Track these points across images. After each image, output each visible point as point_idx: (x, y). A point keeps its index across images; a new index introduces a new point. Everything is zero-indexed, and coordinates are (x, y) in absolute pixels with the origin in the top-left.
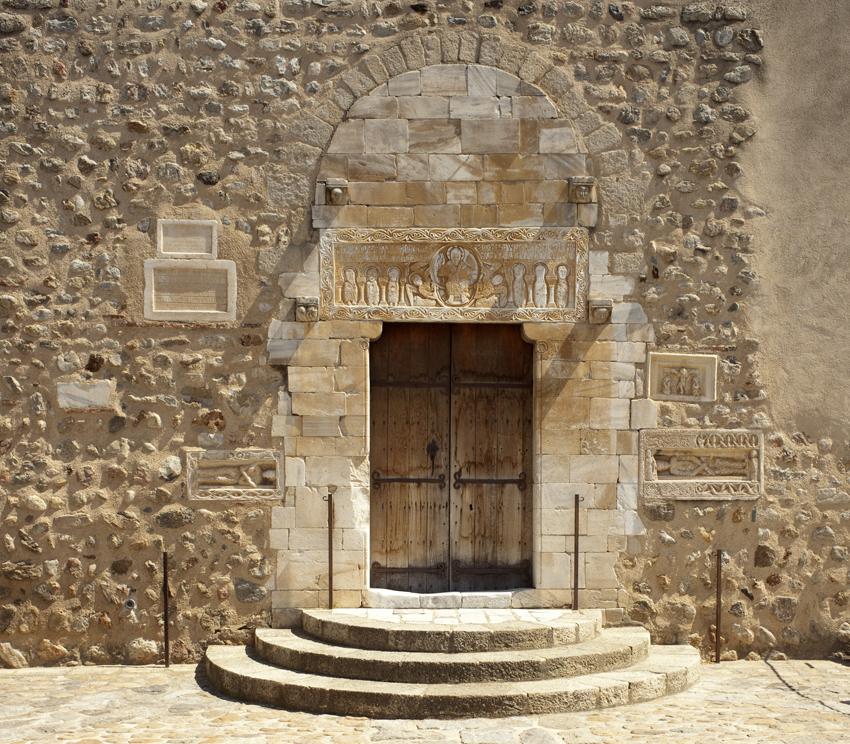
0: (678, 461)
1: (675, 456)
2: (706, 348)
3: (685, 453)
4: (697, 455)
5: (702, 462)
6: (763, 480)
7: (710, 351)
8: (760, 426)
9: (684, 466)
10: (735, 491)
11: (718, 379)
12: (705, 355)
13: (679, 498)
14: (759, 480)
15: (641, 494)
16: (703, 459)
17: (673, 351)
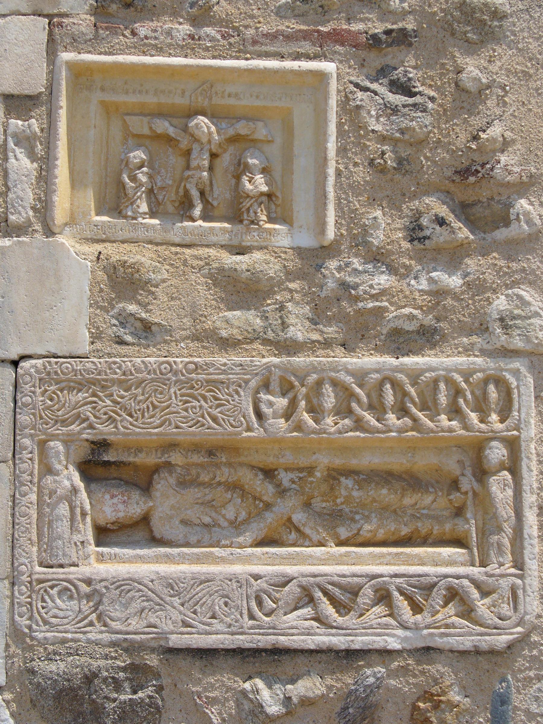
0: (183, 484)
1: (168, 465)
2: (289, 38)
3: (211, 453)
4: (257, 459)
5: (282, 492)
6: (532, 565)
7: (306, 47)
8: (518, 343)
9: (209, 504)
10: (417, 608)
11: (342, 151)
12: (289, 64)
13: (175, 641)
14: (519, 564)
15: (23, 622)
16: (285, 478)
17: (160, 50)
